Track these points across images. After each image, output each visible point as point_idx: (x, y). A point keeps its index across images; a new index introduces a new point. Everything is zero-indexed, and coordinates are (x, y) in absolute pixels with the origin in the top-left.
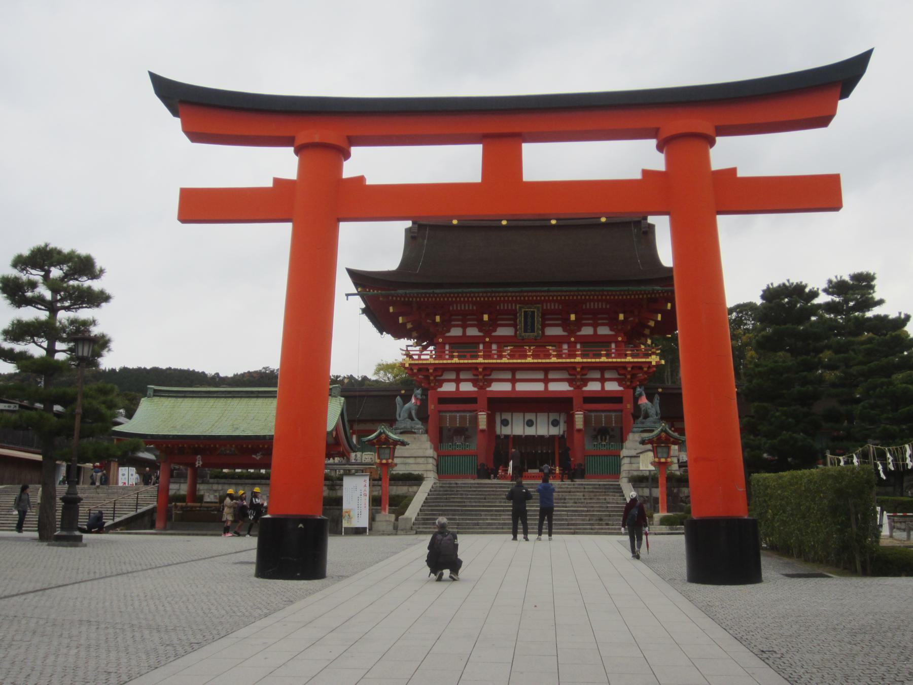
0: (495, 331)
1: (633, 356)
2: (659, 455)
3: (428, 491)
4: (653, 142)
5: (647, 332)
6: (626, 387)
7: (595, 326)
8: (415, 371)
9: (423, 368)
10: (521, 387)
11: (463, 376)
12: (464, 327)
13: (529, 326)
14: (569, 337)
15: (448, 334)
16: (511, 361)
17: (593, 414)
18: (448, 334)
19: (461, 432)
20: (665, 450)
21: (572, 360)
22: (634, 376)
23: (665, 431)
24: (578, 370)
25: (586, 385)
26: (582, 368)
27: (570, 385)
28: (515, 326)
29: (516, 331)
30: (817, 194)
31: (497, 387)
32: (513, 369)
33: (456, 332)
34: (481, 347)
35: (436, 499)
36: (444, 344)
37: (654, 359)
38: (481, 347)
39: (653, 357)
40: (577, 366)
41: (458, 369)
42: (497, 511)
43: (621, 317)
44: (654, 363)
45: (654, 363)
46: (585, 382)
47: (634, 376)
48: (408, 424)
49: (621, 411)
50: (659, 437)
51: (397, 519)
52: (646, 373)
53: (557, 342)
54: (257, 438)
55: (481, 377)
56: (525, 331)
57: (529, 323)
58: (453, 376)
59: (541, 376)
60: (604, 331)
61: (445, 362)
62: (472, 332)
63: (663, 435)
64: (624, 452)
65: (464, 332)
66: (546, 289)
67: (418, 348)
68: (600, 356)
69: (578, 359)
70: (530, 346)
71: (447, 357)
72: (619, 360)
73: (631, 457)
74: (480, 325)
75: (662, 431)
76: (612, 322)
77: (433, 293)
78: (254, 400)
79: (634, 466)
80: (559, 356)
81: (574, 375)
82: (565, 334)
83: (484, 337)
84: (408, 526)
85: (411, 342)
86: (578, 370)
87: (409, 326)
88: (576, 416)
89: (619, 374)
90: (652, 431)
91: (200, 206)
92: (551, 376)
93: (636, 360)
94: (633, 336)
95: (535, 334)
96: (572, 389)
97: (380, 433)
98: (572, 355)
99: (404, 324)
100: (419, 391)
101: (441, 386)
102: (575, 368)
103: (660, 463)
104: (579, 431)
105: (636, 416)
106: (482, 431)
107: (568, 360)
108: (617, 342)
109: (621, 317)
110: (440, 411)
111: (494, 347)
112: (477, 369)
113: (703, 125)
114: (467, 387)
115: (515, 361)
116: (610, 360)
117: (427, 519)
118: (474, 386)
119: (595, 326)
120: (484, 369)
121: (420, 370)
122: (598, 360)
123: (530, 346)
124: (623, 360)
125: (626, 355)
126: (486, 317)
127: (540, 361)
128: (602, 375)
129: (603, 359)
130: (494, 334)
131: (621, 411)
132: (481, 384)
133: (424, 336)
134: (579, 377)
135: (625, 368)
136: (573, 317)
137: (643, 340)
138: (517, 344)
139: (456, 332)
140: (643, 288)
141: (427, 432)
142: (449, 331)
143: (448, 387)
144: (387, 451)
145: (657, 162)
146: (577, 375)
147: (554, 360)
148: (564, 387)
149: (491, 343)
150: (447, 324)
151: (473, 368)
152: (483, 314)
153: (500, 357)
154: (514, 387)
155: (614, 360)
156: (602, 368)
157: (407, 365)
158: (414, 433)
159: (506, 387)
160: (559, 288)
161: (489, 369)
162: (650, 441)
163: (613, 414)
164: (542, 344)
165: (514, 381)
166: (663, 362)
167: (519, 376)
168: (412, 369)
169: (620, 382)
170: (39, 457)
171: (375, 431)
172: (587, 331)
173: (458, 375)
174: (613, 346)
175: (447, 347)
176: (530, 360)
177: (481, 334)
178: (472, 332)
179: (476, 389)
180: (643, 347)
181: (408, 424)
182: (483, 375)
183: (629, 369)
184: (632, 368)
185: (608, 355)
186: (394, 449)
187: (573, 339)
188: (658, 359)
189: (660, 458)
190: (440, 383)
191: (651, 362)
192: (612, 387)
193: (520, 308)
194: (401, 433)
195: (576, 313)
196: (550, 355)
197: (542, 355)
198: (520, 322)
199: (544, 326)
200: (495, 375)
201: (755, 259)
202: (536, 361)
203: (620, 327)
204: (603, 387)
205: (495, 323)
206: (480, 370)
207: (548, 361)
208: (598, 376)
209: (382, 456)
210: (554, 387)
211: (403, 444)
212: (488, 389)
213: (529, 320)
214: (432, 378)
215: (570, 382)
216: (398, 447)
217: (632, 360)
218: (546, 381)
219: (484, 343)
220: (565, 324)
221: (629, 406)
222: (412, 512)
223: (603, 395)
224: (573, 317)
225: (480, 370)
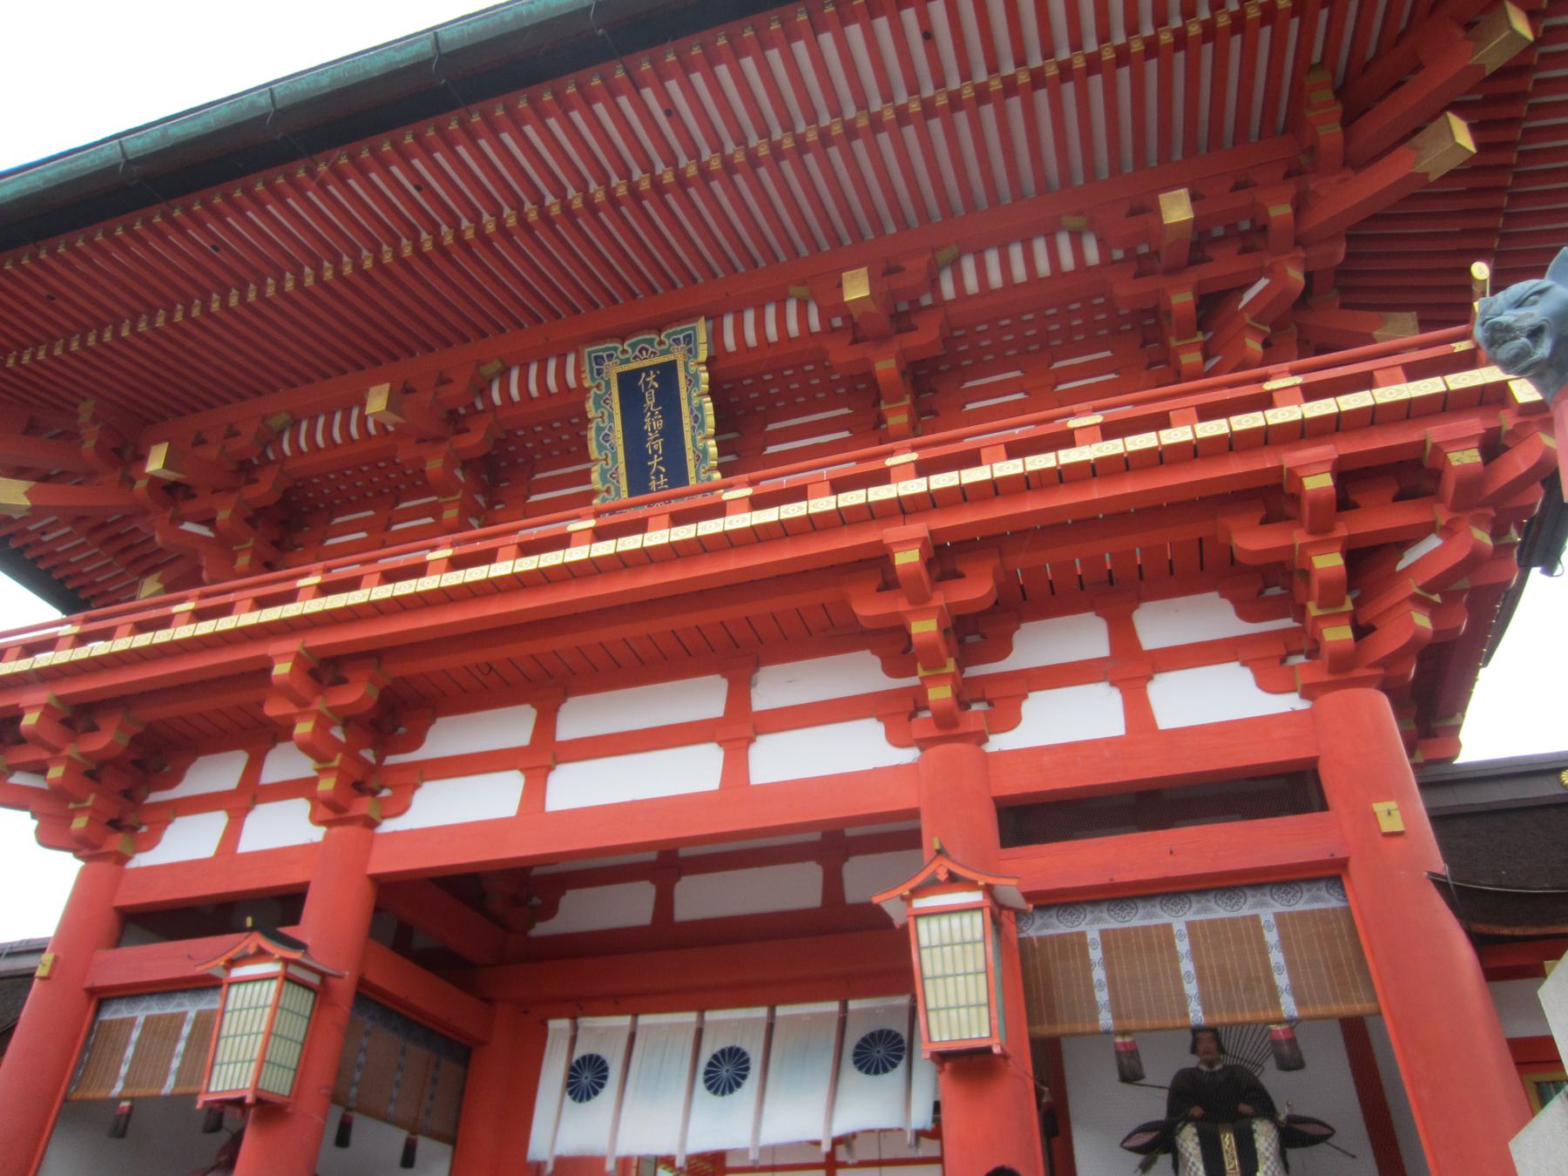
17: (1092, 927)
22: (1368, 561)
27: (896, 738)
57: (655, 444)
59: (703, 699)
88: (927, 933)
96: (909, 755)
128: (1122, 634)
148: (860, 751)
159: (492, 799)
163: (1266, 910)
192: (1214, 701)
204: (1138, 710)
210: (779, 760)
213: (653, 424)
218: (737, 730)
221: (1389, 816)
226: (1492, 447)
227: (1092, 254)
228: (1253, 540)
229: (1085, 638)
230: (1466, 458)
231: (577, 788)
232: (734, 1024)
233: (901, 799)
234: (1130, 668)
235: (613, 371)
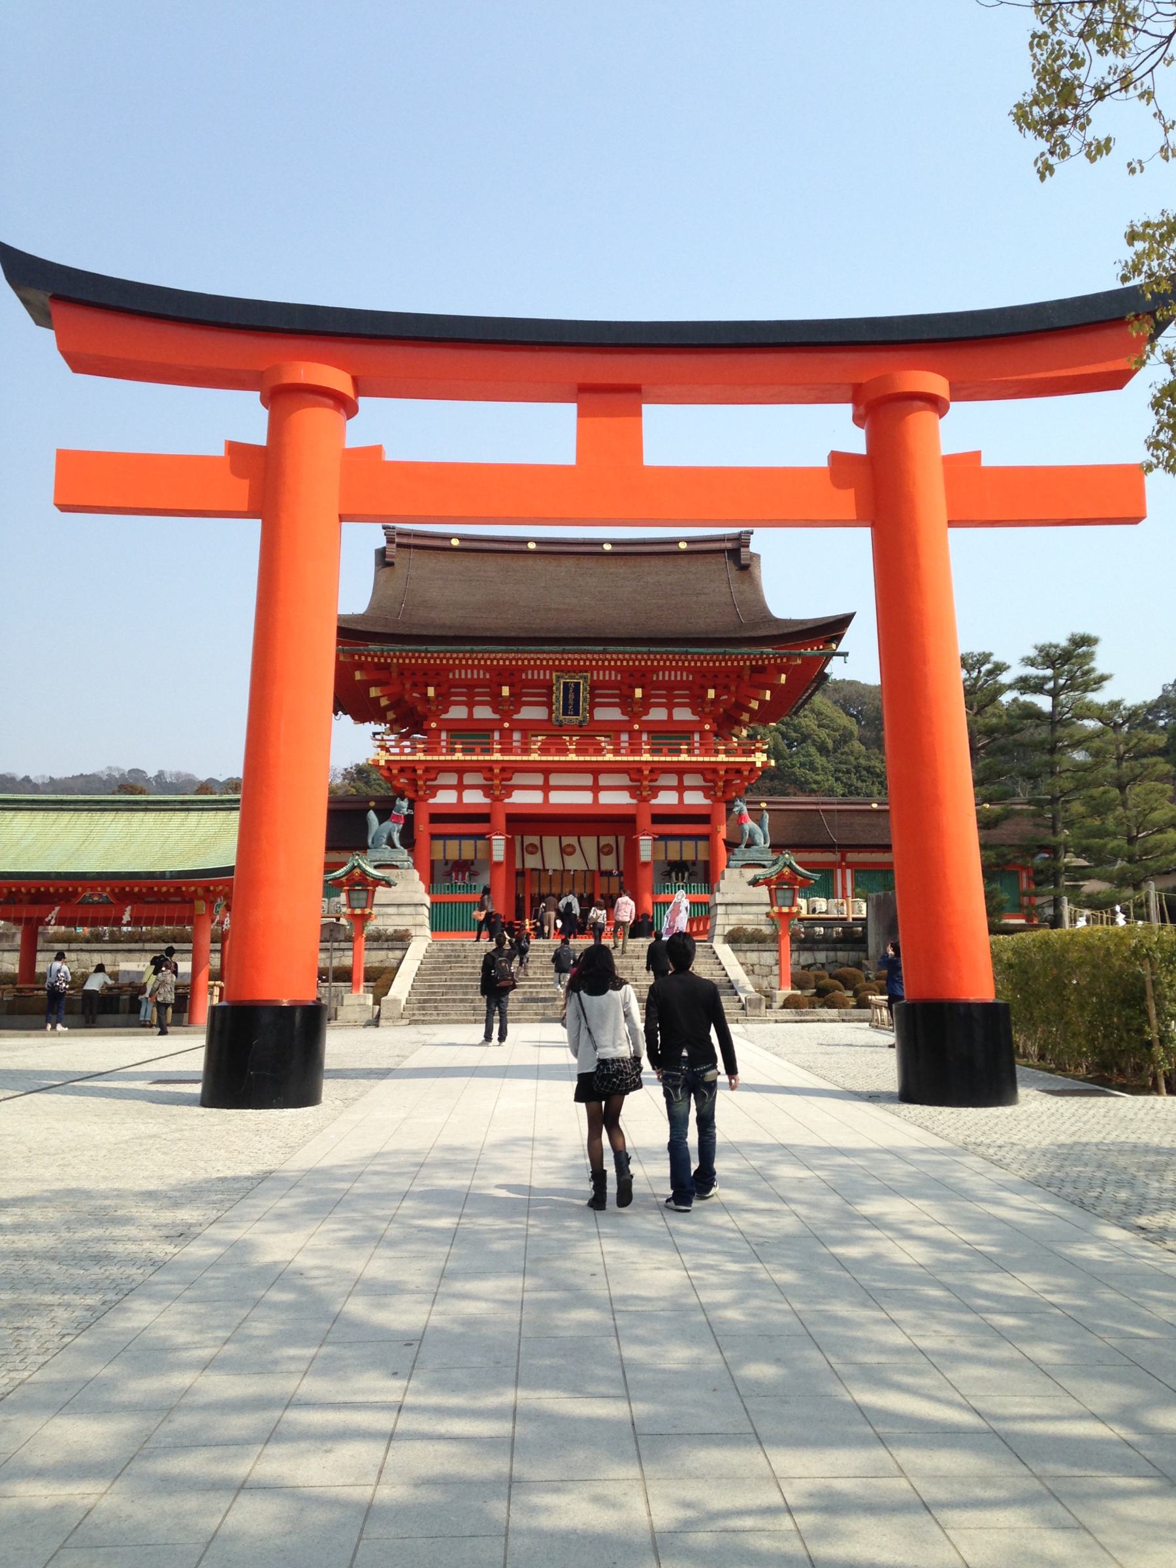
0: (518, 712)
1: (727, 752)
2: (780, 901)
3: (421, 957)
4: (847, 409)
5: (745, 717)
6: (716, 800)
7: (670, 707)
8: (395, 772)
9: (407, 769)
10: (556, 798)
11: (469, 779)
12: (470, 705)
13: (572, 707)
14: (631, 722)
15: (444, 716)
16: (544, 758)
18: (444, 716)
19: (462, 866)
20: (789, 894)
21: (637, 758)
22: (728, 783)
23: (790, 866)
24: (646, 772)
25: (655, 797)
26: (651, 771)
28: (549, 705)
29: (551, 712)
30: (1100, 499)
31: (521, 798)
32: (546, 770)
33: (457, 712)
34: (497, 736)
35: (434, 969)
36: (439, 730)
37: (759, 759)
38: (497, 736)
39: (758, 754)
40: (644, 767)
41: (461, 769)
42: (530, 986)
43: (711, 694)
44: (759, 765)
45: (759, 765)
46: (655, 791)
47: (728, 783)
48: (385, 854)
49: (706, 837)
50: (780, 875)
51: (377, 1002)
52: (748, 779)
53: (612, 730)
54: (151, 875)
55: (496, 782)
56: (565, 713)
58: (452, 779)
59: (588, 780)
60: (683, 714)
61: (442, 758)
62: (483, 713)
63: (786, 870)
64: (719, 898)
65: (471, 713)
66: (601, 648)
67: (393, 737)
68: (679, 752)
69: (646, 757)
70: (571, 736)
71: (444, 750)
72: (707, 759)
73: (727, 904)
74: (496, 702)
75: (785, 865)
76: (697, 702)
77: (427, 651)
78: (141, 814)
79: (733, 919)
80: (616, 752)
81: (638, 781)
82: (626, 718)
83: (502, 721)
84: (396, 1014)
85: (381, 728)
86: (646, 772)
87: (384, 702)
88: (641, 843)
89: (705, 780)
90: (764, 866)
91: (95, 486)
92: (604, 780)
93: (732, 759)
94: (726, 723)
95: (580, 718)
96: (634, 801)
97: (354, 867)
98: (635, 750)
99: (377, 699)
100: (405, 804)
101: (434, 796)
102: (640, 771)
103: (780, 914)
104: (646, 864)
105: (731, 845)
106: (499, 864)
107: (631, 759)
108: (702, 733)
109: (711, 694)
110: (434, 837)
111: (517, 736)
112: (491, 770)
113: (937, 384)
114: (474, 798)
115: (550, 758)
116: (694, 759)
117: (425, 1001)
118: (486, 795)
119: (670, 707)
120: (503, 770)
121: (402, 770)
122: (675, 759)
123: (571, 736)
124: (713, 759)
125: (717, 752)
126: (506, 691)
127: (588, 758)
128: (681, 781)
129: (684, 757)
130: (516, 717)
131: (706, 837)
132: (497, 793)
133: (407, 718)
134: (646, 783)
135: (715, 771)
136: (638, 693)
137: (736, 730)
138: (553, 733)
139: (457, 712)
140: (745, 650)
141: (416, 866)
142: (446, 712)
143: (445, 798)
144: (363, 895)
145: (856, 441)
146: (641, 780)
147: (609, 757)
149: (511, 730)
150: (444, 701)
151: (486, 769)
152: (501, 685)
153: (526, 751)
154: (546, 797)
155: (700, 759)
156: (680, 770)
157: (382, 763)
158: (396, 867)
159: (536, 797)
160: (621, 648)
161: (509, 769)
162: (767, 882)
164: (589, 734)
165: (546, 788)
166: (773, 763)
167: (555, 780)
168: (389, 769)
169: (707, 791)
170: (1023, 921)
171: (344, 864)
172: (657, 714)
173: (460, 779)
174: (697, 737)
175: (444, 736)
176: (572, 757)
177: (497, 716)
178: (483, 713)
179: (488, 801)
180: (735, 739)
181: (385, 854)
182: (498, 780)
183: (722, 773)
184: (726, 772)
185: (690, 752)
186: (374, 892)
187: (636, 727)
188: (764, 757)
189: (780, 907)
190: (434, 790)
191: (754, 763)
192: (695, 799)
193: (558, 678)
194: (376, 867)
195: (642, 687)
196: (603, 749)
197: (591, 749)
198: (558, 698)
199: (593, 705)
200: (518, 779)
201: (1004, 598)
202: (581, 758)
203: (707, 710)
204: (681, 798)
205: (517, 701)
206: (497, 771)
207: (600, 759)
208: (675, 783)
209: (355, 904)
210: (606, 798)
211: (389, 884)
212: (506, 801)
213: (571, 696)
214: (420, 783)
215: (633, 791)
216: (380, 889)
217: (726, 759)
218: (596, 789)
219: (502, 730)
220: (626, 701)
222: (401, 988)
223: (682, 812)
224: (638, 693)
225: (497, 771)
226: (751, 771)
227: (691, 678)
228: (709, 777)
229: (673, 780)
230: (746, 773)
231: (556, 798)
232: (566, 840)
233: (632, 812)
234: (681, 789)
235: (562, 681)
